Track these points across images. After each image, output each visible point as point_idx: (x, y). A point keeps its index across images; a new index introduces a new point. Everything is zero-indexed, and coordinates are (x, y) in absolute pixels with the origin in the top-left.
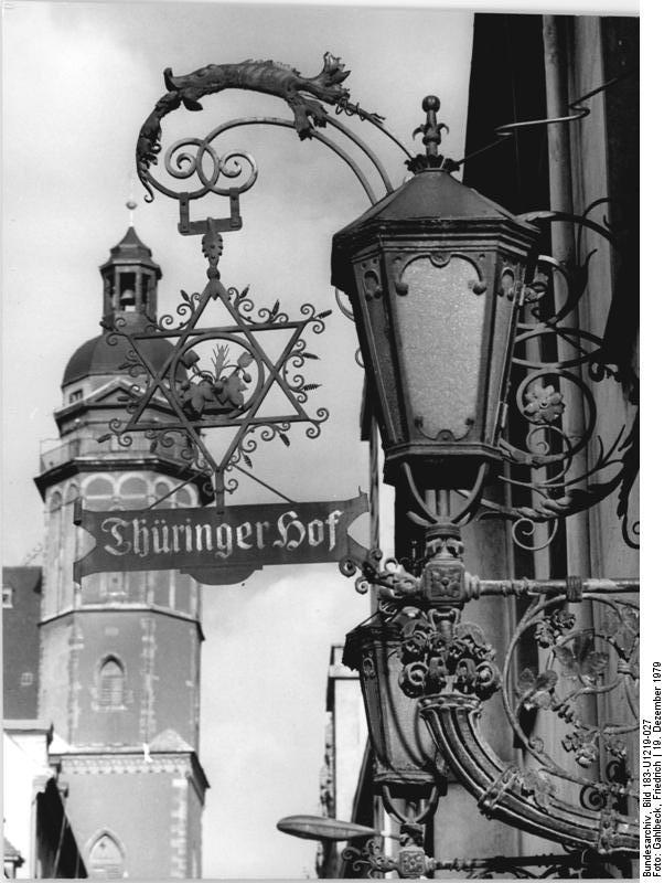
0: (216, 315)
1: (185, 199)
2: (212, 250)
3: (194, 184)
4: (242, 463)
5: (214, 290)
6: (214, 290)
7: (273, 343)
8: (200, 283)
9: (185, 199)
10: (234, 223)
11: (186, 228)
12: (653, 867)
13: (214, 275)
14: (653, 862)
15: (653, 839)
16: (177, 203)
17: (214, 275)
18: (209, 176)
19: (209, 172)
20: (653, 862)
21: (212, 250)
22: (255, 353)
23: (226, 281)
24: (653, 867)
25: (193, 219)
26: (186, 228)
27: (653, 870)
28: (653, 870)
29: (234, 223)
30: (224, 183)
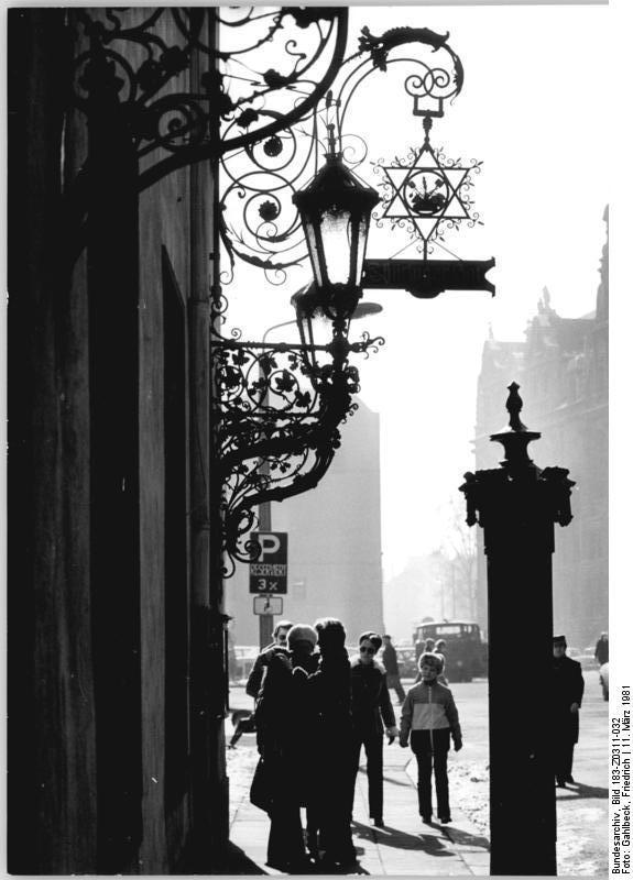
0: (427, 160)
1: (416, 97)
2: (427, 125)
3: (421, 91)
4: (438, 240)
5: (427, 147)
6: (427, 147)
7: (454, 177)
8: (422, 143)
9: (416, 97)
10: (440, 114)
11: (417, 112)
12: (622, 865)
13: (427, 139)
14: (622, 859)
15: (622, 836)
16: (412, 99)
17: (427, 139)
18: (428, 88)
19: (429, 86)
20: (622, 859)
21: (427, 125)
22: (445, 181)
23: (432, 144)
24: (622, 865)
25: (420, 108)
26: (417, 112)
27: (622, 867)
28: (622, 867)
29: (440, 114)
30: (437, 91)
